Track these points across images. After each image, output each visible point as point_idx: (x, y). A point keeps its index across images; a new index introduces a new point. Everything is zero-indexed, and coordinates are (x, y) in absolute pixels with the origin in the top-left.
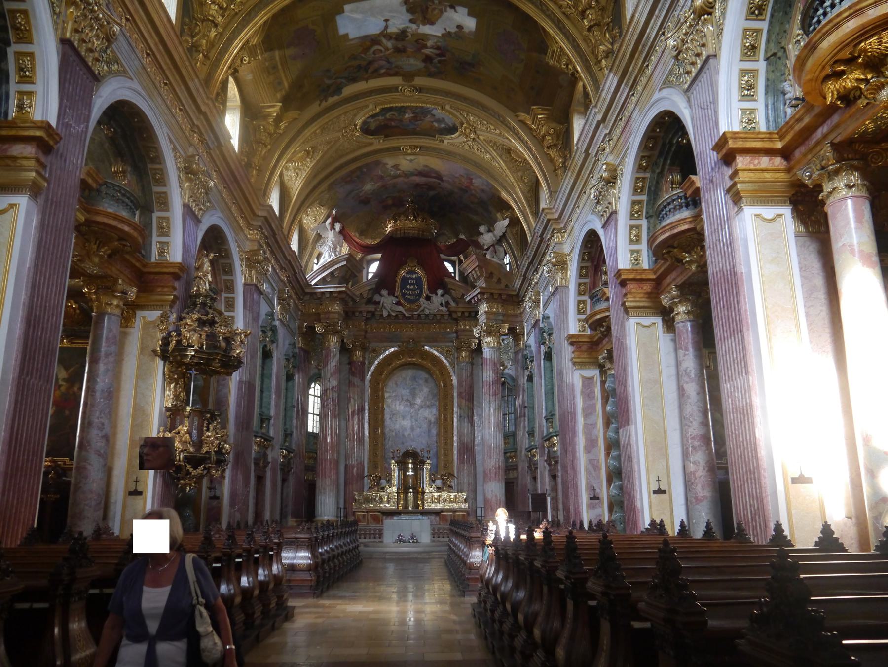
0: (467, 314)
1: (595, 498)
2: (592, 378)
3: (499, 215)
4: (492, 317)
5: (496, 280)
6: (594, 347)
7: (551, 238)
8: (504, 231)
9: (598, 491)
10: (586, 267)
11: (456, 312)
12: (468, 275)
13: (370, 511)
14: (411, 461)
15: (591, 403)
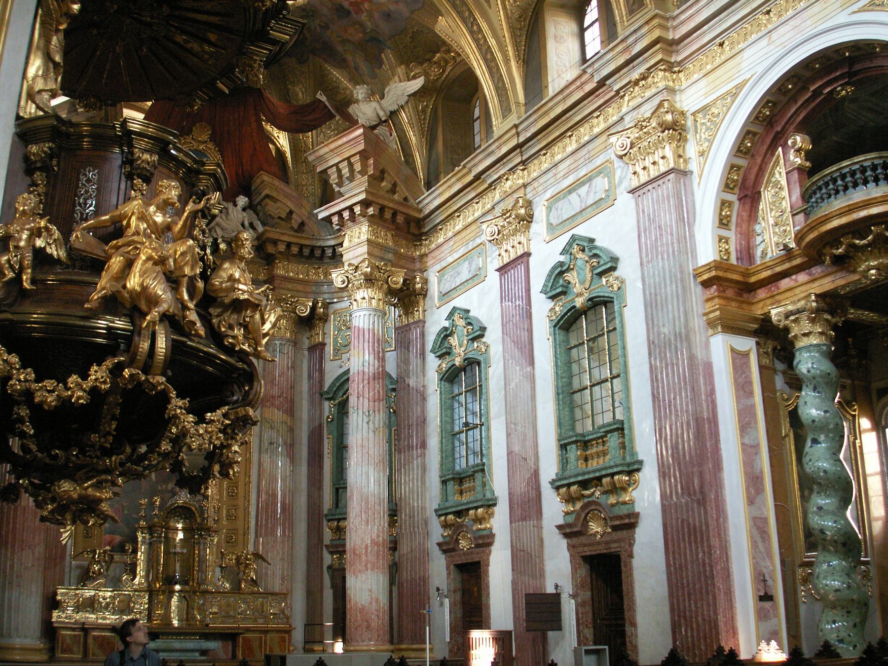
0: (295, 250)
1: (766, 597)
2: (746, 355)
3: (401, 70)
4: (377, 252)
5: (390, 186)
6: (745, 295)
7: (636, 83)
8: (402, 102)
9: (770, 582)
10: (755, 134)
11: (275, 242)
12: (325, 171)
13: (94, 629)
14: (180, 526)
15: (749, 403)
